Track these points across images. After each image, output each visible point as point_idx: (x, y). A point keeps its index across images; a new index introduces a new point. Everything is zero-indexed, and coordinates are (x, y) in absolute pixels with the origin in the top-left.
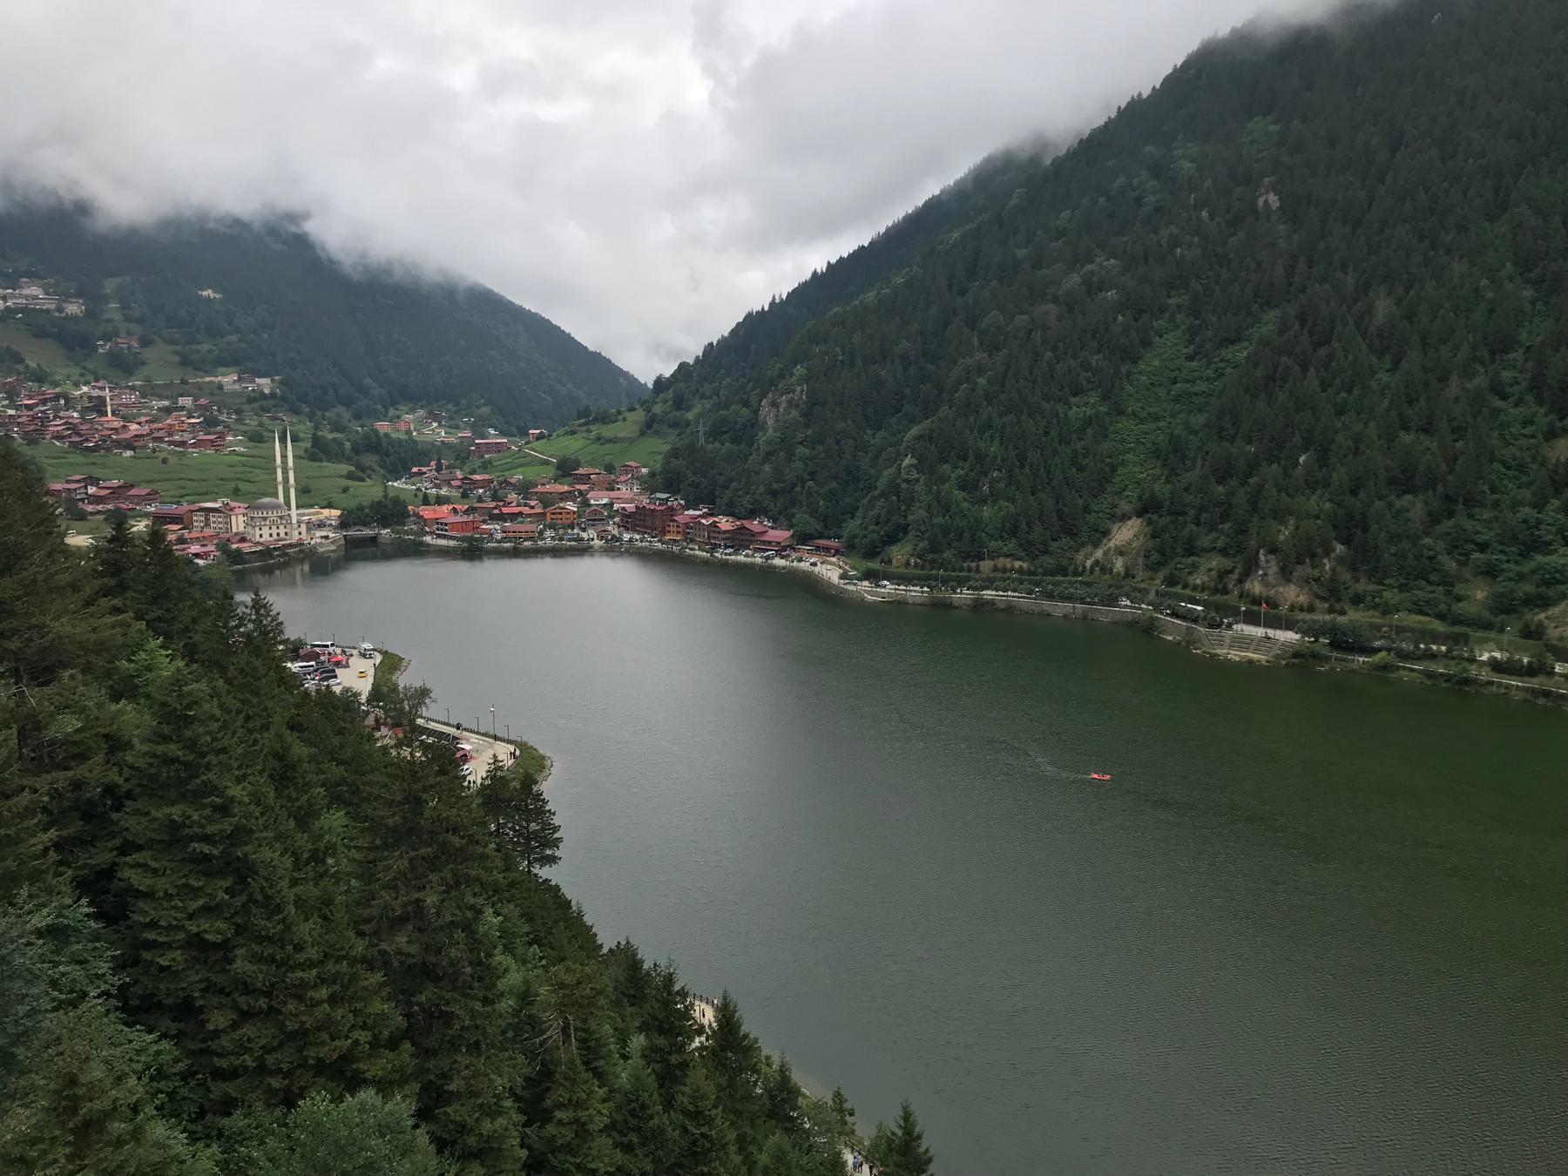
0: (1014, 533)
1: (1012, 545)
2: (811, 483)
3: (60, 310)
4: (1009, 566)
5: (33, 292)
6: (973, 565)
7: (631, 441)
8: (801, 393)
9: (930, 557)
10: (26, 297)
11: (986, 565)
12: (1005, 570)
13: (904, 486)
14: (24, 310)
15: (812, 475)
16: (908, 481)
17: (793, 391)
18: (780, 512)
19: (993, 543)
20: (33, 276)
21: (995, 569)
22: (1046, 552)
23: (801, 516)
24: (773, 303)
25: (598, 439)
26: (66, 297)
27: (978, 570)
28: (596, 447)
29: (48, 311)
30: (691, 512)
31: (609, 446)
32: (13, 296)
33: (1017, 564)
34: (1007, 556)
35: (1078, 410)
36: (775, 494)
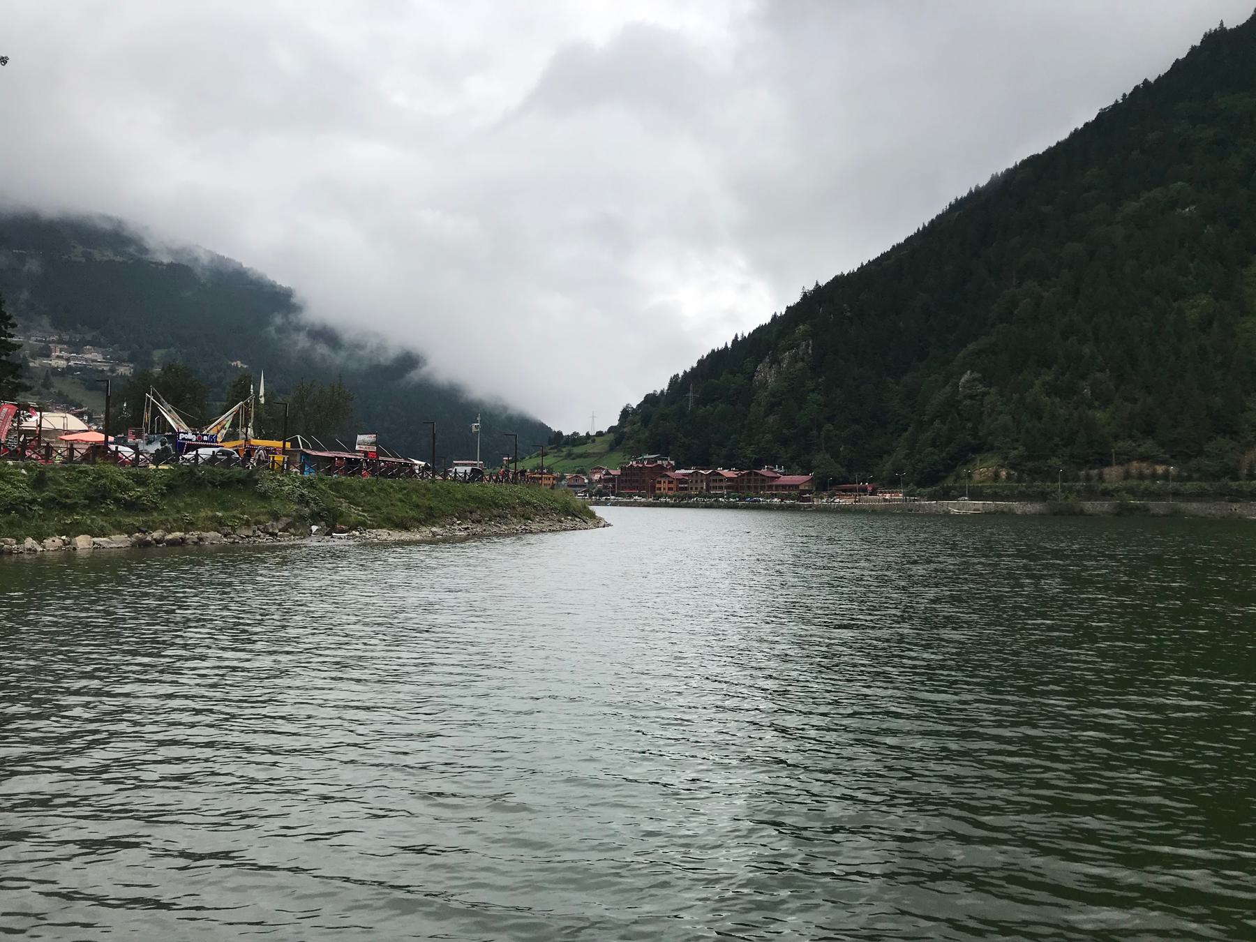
0: (1149, 430)
1: (1148, 446)
2: (829, 426)
3: (112, 370)
4: (1147, 472)
5: (94, 357)
6: (1094, 472)
7: (600, 455)
8: (806, 348)
9: (1030, 465)
10: (86, 360)
11: (1113, 473)
12: (1141, 477)
13: (968, 402)
14: (82, 369)
15: (829, 419)
16: (971, 397)
17: (798, 346)
18: (792, 459)
19: (1121, 444)
20: (95, 344)
21: (1127, 476)
22: (1200, 453)
23: (821, 458)
24: (735, 341)
25: (569, 455)
26: (121, 361)
27: (1101, 478)
28: (568, 463)
29: (103, 371)
30: (683, 471)
31: (578, 460)
32: (75, 359)
33: (1160, 469)
34: (1143, 458)
35: (1199, 305)
36: (785, 442)
